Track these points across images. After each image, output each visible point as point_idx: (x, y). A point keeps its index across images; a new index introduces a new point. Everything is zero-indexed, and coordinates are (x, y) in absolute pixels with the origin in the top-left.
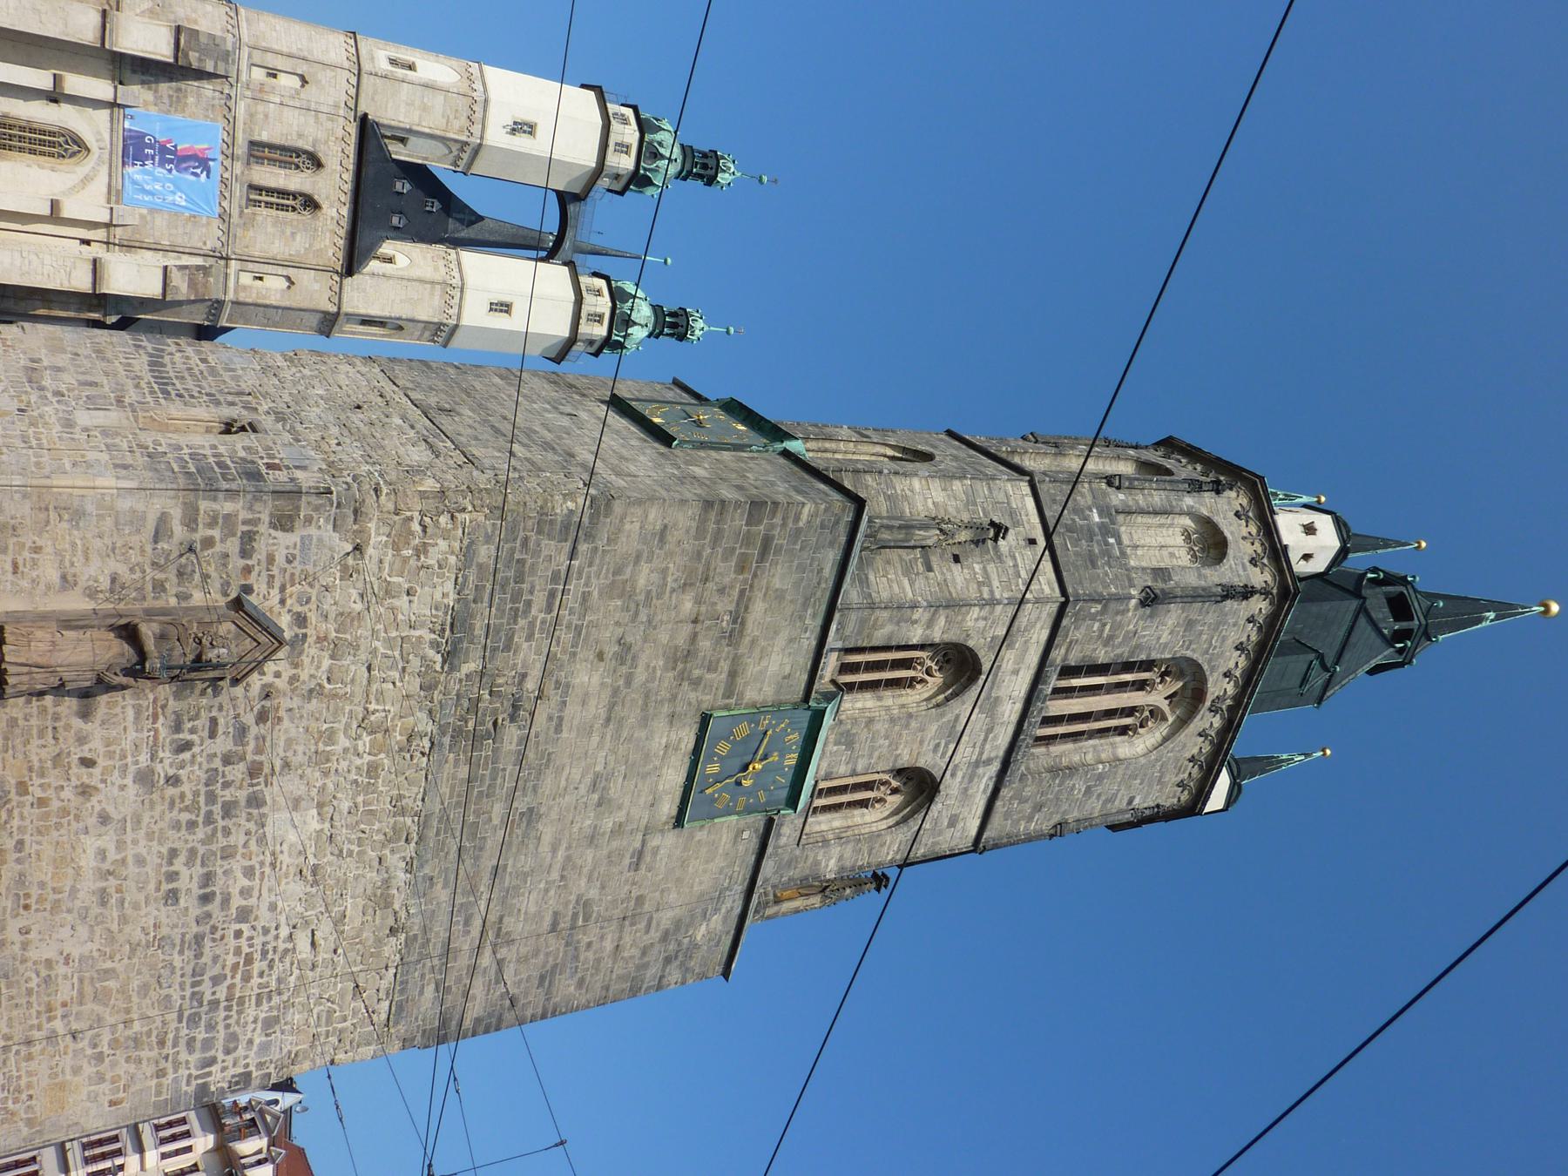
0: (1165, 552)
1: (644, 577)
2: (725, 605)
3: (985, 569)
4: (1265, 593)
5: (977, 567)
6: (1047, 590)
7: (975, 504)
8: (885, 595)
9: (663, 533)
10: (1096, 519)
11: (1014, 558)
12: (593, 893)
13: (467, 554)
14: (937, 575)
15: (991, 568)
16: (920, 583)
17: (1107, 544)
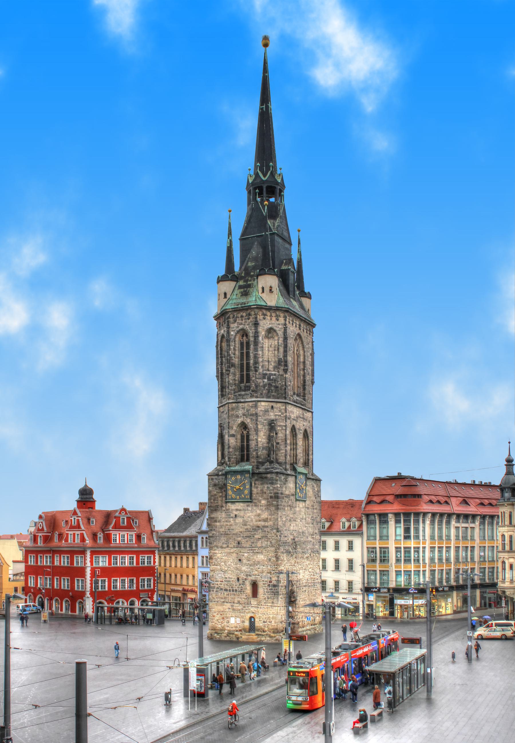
0: (270, 349)
1: (284, 519)
2: (287, 500)
3: (279, 426)
4: (285, 317)
5: (279, 428)
6: (284, 407)
7: (263, 423)
8: (284, 458)
9: (281, 517)
10: (266, 380)
11: (276, 415)
12: (310, 516)
13: (283, 553)
14: (280, 441)
15: (279, 424)
16: (282, 447)
17: (272, 380)
